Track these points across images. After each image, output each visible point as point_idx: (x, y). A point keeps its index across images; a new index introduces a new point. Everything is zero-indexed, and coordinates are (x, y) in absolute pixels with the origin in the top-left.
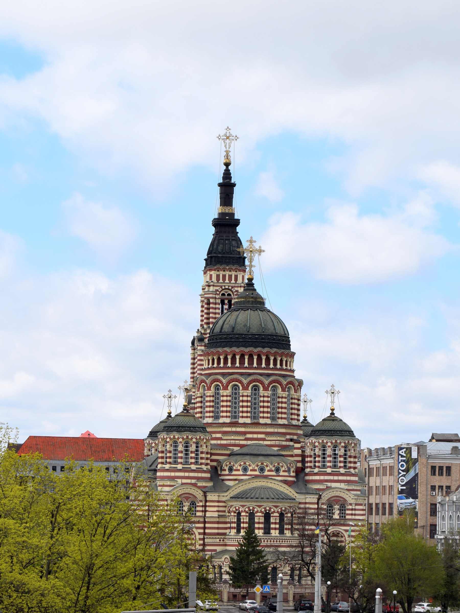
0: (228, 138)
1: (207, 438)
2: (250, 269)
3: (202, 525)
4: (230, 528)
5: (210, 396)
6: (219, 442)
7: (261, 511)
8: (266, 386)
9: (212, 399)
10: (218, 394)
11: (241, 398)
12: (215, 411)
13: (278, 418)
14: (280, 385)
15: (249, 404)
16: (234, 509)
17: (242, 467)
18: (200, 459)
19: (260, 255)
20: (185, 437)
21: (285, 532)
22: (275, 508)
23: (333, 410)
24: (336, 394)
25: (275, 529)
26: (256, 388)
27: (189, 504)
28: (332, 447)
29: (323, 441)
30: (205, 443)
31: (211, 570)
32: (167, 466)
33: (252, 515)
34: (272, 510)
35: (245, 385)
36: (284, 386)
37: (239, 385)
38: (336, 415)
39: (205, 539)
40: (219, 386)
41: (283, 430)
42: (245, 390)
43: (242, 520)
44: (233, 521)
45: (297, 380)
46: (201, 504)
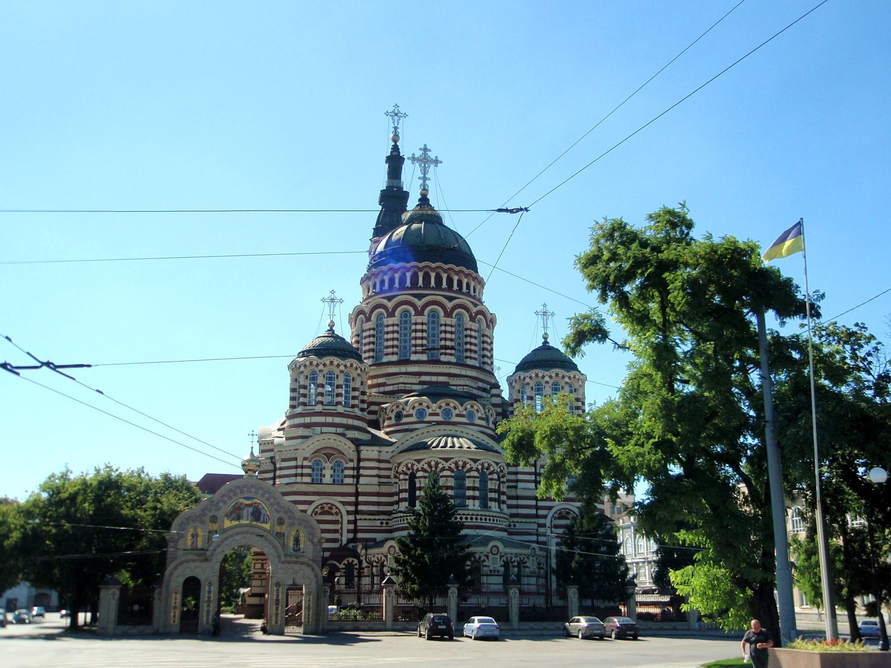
0: (396, 114)
1: (363, 369)
2: (424, 182)
3: (353, 499)
4: (397, 503)
5: (370, 329)
6: (382, 389)
7: (449, 467)
9: (372, 332)
10: (381, 325)
11: (413, 327)
13: (467, 357)
14: (468, 312)
15: (425, 335)
16: (405, 469)
17: (416, 409)
18: (352, 399)
19: (436, 166)
20: (328, 363)
21: (489, 505)
22: (472, 463)
23: (545, 338)
24: (550, 317)
25: (474, 498)
26: (434, 315)
27: (331, 465)
28: (550, 384)
29: (537, 375)
30: (359, 375)
31: (366, 569)
32: (299, 410)
34: (468, 466)
35: (419, 308)
36: (474, 314)
37: (411, 309)
38: (551, 345)
41: (473, 373)
43: (418, 485)
44: (404, 488)
45: (491, 314)
46: (351, 465)
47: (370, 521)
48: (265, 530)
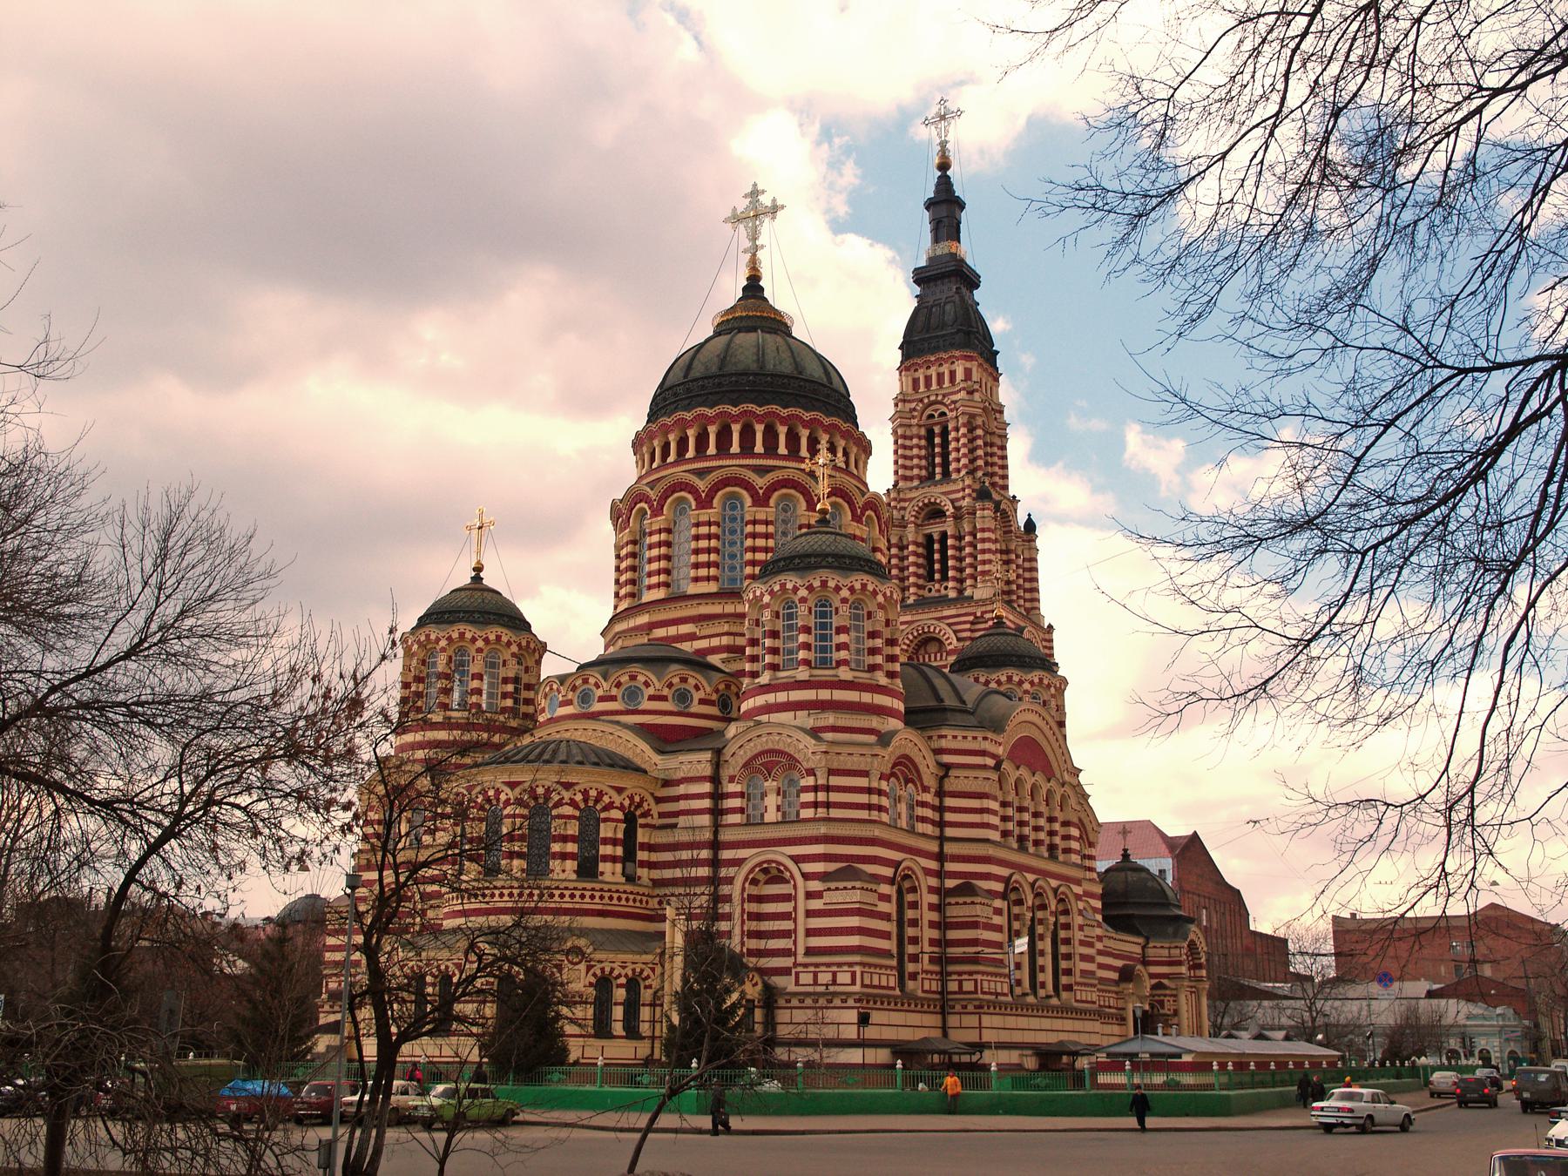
0: (943, 118)
8: (761, 492)
26: (733, 501)
33: (589, 819)
42: (703, 508)
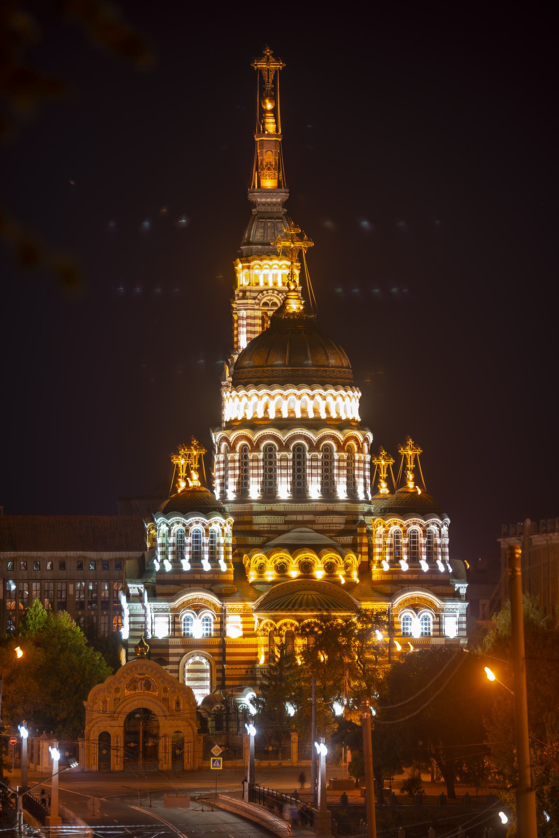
12: (242, 482)
31: (233, 714)
39: (226, 671)
40: (247, 446)
47: (236, 670)
48: (154, 697)
